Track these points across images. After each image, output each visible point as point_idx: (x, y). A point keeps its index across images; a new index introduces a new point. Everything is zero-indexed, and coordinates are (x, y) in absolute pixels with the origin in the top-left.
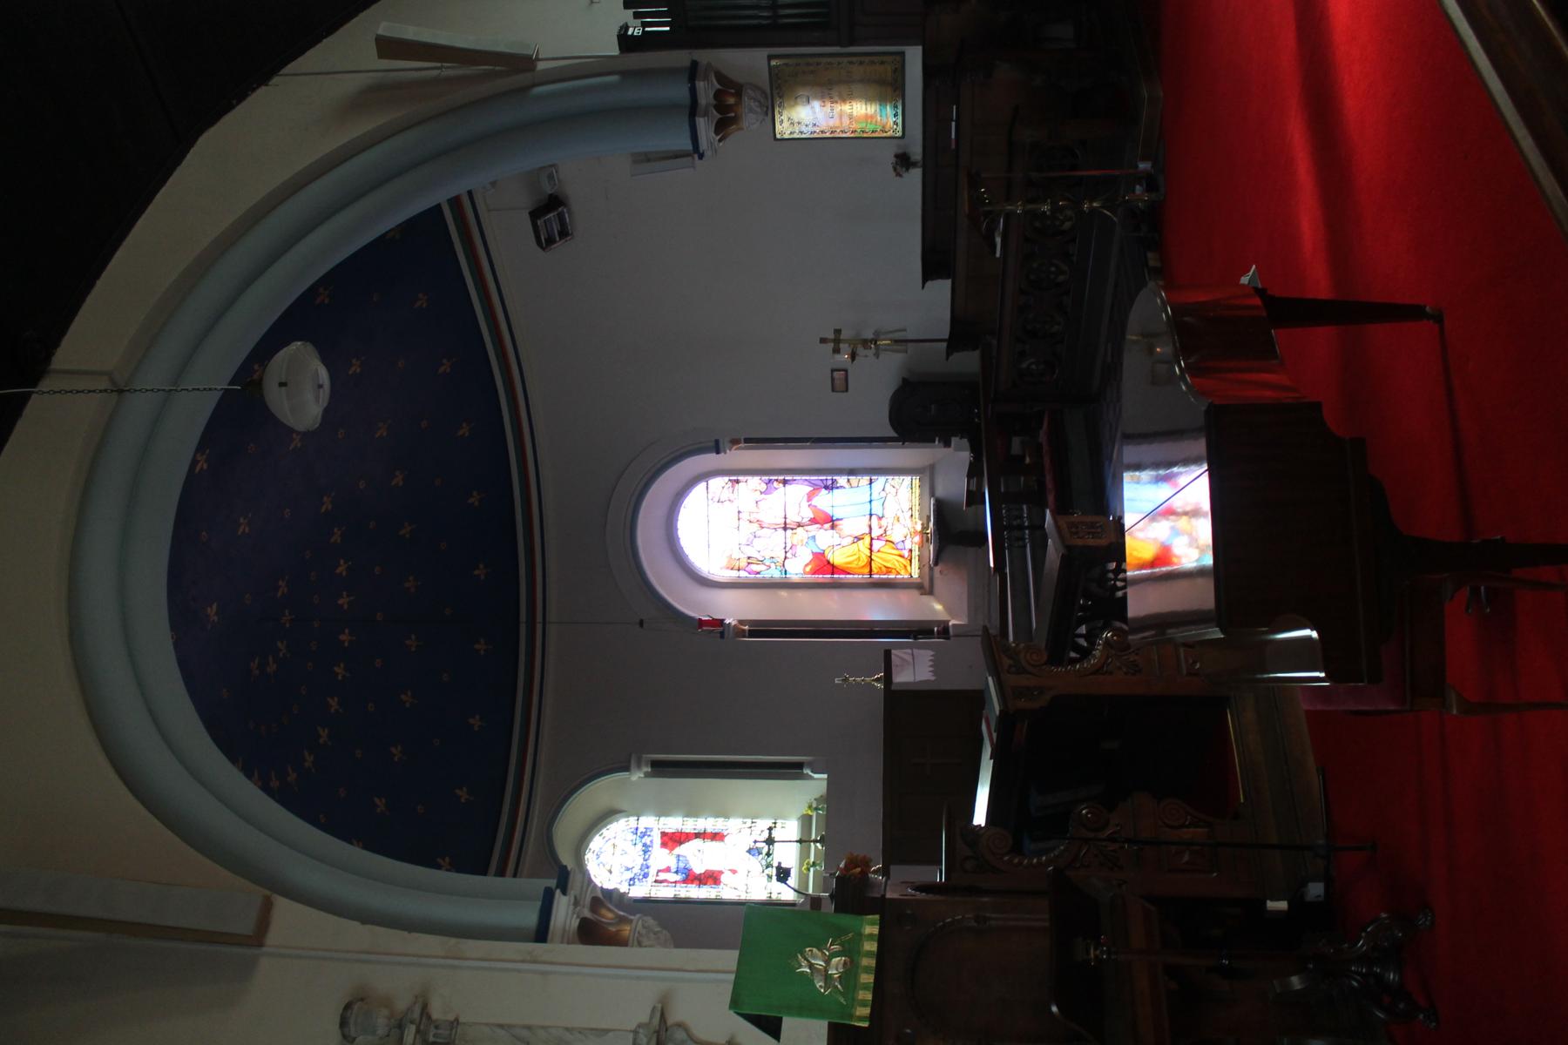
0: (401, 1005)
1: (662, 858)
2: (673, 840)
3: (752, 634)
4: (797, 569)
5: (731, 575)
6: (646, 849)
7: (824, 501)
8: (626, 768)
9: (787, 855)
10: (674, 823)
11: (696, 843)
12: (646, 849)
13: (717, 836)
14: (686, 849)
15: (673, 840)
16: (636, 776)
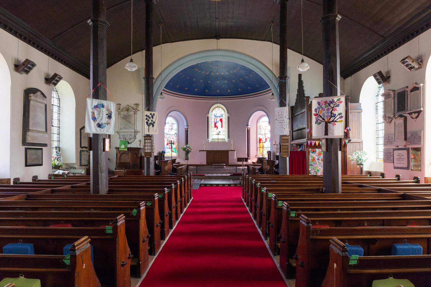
0: (138, 109)
1: (218, 119)
2: (221, 120)
3: (248, 130)
4: (260, 136)
5: (258, 126)
6: (220, 117)
7: (268, 140)
8: (228, 113)
9: (216, 137)
10: (223, 120)
11: (221, 124)
12: (220, 117)
13: (222, 127)
14: (220, 122)
15: (221, 120)
16: (227, 115)
